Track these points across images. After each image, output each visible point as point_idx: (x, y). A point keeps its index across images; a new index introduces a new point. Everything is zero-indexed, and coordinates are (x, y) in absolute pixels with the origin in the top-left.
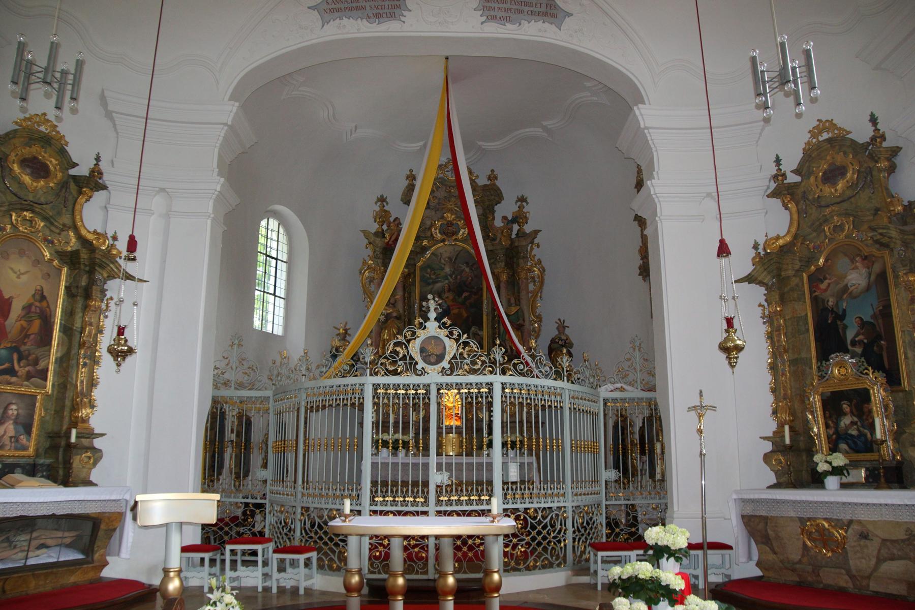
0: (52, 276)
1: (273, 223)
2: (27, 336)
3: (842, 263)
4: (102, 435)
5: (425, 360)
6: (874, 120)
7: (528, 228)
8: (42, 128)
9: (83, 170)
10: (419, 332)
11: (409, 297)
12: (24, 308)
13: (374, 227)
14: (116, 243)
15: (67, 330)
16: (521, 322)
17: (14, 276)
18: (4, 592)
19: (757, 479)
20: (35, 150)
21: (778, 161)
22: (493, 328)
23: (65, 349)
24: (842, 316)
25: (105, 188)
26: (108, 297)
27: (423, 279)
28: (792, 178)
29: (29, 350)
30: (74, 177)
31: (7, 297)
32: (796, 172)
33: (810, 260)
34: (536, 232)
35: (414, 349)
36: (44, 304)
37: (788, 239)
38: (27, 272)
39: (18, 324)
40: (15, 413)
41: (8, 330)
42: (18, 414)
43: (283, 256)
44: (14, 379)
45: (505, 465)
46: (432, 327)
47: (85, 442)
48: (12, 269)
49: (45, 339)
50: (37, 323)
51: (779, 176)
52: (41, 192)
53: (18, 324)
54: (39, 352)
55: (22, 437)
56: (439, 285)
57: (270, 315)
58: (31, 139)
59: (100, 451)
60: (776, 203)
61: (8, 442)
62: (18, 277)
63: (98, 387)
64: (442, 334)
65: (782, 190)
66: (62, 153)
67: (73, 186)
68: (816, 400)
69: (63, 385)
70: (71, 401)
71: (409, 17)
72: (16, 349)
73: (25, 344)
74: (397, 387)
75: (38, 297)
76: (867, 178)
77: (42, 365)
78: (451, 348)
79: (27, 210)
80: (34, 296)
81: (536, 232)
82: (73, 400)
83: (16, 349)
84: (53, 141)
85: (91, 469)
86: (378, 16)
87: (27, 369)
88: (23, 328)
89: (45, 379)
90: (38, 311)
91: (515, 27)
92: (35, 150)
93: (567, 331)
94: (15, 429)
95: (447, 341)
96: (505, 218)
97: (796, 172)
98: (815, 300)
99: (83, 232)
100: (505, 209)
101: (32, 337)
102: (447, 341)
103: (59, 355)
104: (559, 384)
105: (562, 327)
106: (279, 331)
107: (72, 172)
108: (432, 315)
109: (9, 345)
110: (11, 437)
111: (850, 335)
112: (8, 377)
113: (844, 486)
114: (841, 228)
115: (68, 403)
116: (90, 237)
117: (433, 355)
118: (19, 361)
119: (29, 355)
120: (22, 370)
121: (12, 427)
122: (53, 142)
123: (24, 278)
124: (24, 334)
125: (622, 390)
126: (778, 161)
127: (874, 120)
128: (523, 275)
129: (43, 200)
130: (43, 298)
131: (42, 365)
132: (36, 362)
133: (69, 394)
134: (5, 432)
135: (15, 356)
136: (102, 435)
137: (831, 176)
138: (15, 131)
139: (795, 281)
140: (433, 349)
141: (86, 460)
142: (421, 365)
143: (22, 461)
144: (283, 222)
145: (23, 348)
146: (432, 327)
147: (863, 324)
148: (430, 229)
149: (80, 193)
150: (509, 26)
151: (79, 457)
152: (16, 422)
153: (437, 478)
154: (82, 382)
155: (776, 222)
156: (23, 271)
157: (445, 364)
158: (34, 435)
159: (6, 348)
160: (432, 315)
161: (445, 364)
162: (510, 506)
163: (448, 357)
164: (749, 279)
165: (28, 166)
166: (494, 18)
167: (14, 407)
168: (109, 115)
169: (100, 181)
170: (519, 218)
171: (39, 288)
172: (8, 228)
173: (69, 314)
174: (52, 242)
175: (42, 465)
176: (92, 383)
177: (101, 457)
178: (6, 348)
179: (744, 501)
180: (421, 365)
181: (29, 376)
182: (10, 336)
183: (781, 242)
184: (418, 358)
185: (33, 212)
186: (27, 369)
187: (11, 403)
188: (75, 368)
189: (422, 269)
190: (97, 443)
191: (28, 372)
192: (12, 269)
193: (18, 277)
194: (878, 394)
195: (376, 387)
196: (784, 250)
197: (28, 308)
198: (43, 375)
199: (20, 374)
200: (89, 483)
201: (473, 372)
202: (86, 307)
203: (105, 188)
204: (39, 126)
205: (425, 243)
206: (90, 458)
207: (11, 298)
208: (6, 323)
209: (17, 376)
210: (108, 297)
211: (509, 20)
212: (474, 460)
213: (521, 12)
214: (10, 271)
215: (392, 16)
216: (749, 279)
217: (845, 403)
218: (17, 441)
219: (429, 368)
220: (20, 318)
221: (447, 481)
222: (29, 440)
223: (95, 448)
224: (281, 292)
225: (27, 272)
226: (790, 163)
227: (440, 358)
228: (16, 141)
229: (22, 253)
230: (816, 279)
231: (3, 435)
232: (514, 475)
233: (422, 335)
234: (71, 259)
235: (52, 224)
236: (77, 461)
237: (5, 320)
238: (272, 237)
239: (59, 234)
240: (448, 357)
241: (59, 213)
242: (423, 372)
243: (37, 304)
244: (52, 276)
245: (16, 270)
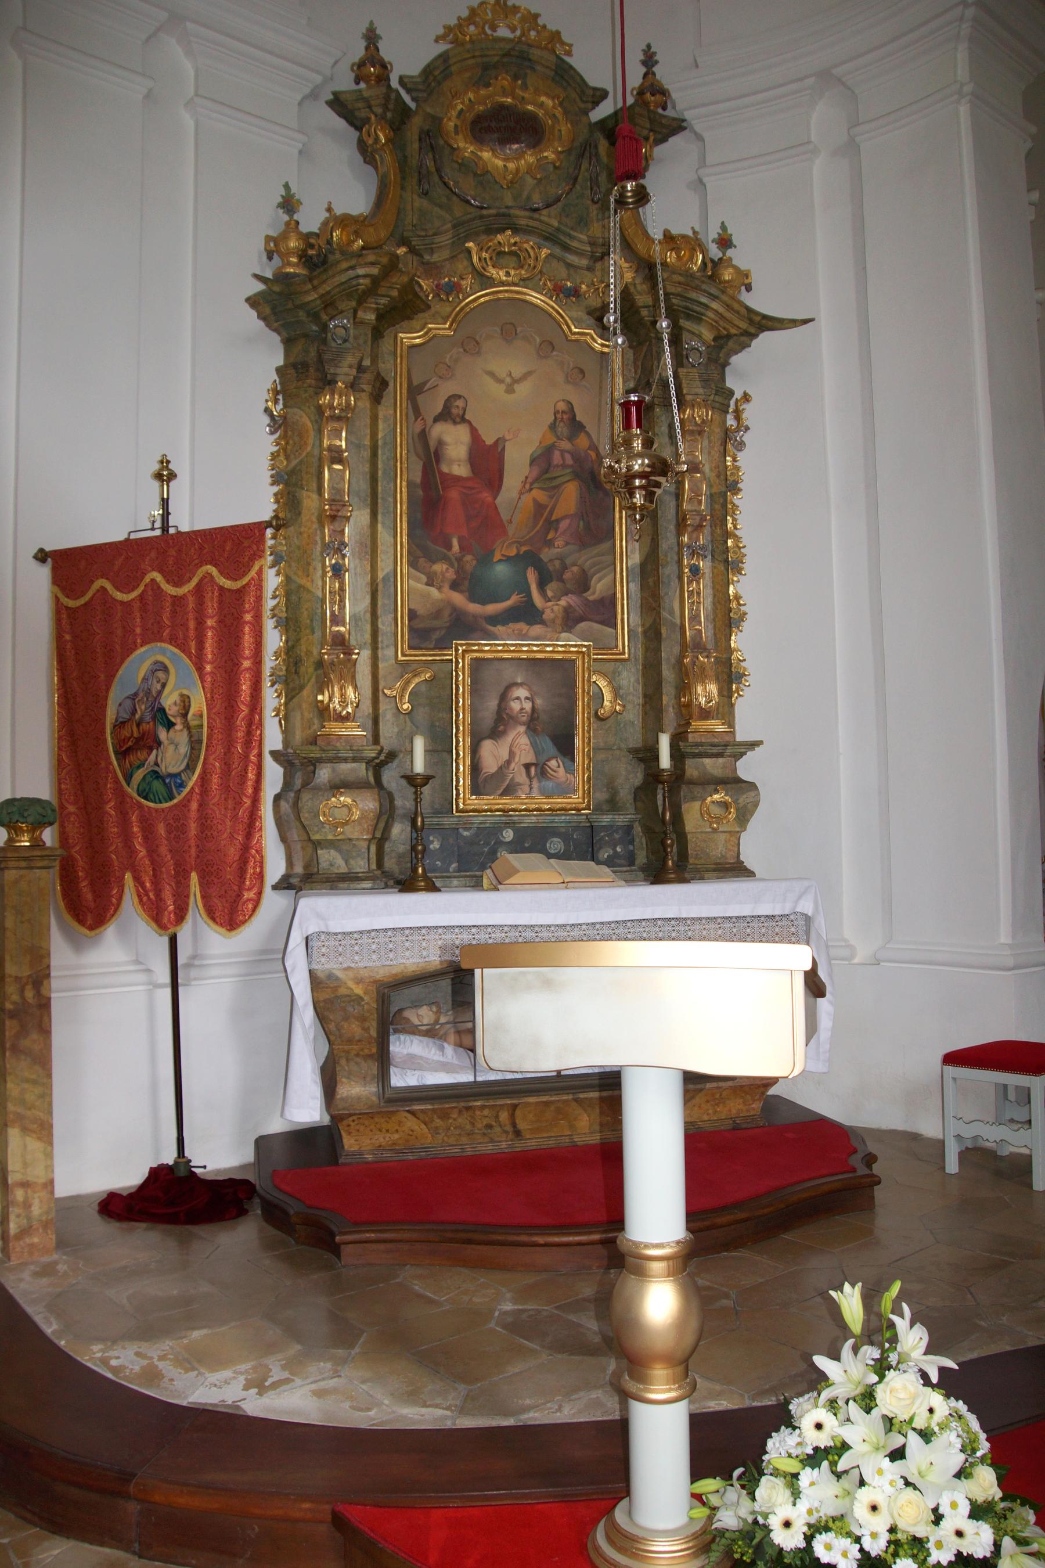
2: (551, 524)
4: (754, 745)
8: (503, 32)
12: (533, 461)
14: (730, 253)
17: (497, 390)
18: (518, 1133)
23: (647, 540)
25: (678, 126)
26: (738, 395)
29: (561, 558)
31: (489, 441)
36: (582, 442)
38: (525, 377)
39: (527, 499)
40: (528, 706)
41: (505, 516)
42: (533, 709)
44: (537, 629)
47: (712, 766)
48: (491, 374)
50: (571, 495)
52: (530, 181)
53: (527, 499)
54: (586, 558)
55: (553, 763)
58: (486, 67)
59: (752, 786)
61: (521, 777)
62: (510, 390)
63: (745, 625)
66: (564, 75)
69: (652, 635)
70: (685, 668)
72: (530, 559)
73: (550, 544)
75: (563, 429)
77: (598, 588)
79: (502, 230)
80: (553, 427)
82: (680, 662)
83: (530, 559)
84: (535, 53)
85: (736, 836)
87: (563, 603)
88: (539, 507)
89: (610, 621)
90: (569, 461)
92: (501, 92)
94: (534, 745)
101: (564, 525)
103: (636, 559)
109: (513, 552)
110: (527, 766)
112: (522, 626)
115: (668, 673)
118: (542, 585)
119: (565, 568)
120: (553, 609)
121: (524, 741)
123: (523, 389)
124: (544, 519)
129: (537, 201)
130: (576, 427)
131: (598, 588)
132: (583, 584)
133: (669, 651)
134: (512, 754)
135: (532, 576)
136: (754, 745)
138: (444, 57)
141: (716, 811)
143: (560, 820)
145: (546, 555)
151: (697, 805)
152: (533, 724)
154: (695, 618)
156: (517, 373)
158: (579, 758)
159: (508, 559)
165: (489, 130)
167: (522, 693)
169: (670, 112)
171: (562, 406)
172: (467, 283)
174: (575, 292)
175: (610, 828)
176: (727, 617)
177: (756, 805)
178: (508, 559)
181: (570, 621)
182: (511, 530)
185: (516, 230)
186: (563, 603)
187: (516, 684)
188: (675, 583)
190: (746, 768)
191: (567, 610)
192: (491, 374)
193: (510, 390)
197: (543, 460)
198: (604, 611)
199: (548, 615)
200: (735, 869)
203: (678, 126)
204: (494, 28)
206: (726, 805)
207: (500, 442)
208: (498, 501)
209: (543, 622)
210: (738, 395)
214: (488, 379)
218: (543, 773)
220: (528, 485)
222: (570, 771)
223: (739, 781)
225: (525, 377)
229: (509, 333)
231: (508, 762)
235: (566, 248)
236: (693, 816)
237: (495, 498)
239: (589, 269)
243: (565, 445)
245: (502, 373)
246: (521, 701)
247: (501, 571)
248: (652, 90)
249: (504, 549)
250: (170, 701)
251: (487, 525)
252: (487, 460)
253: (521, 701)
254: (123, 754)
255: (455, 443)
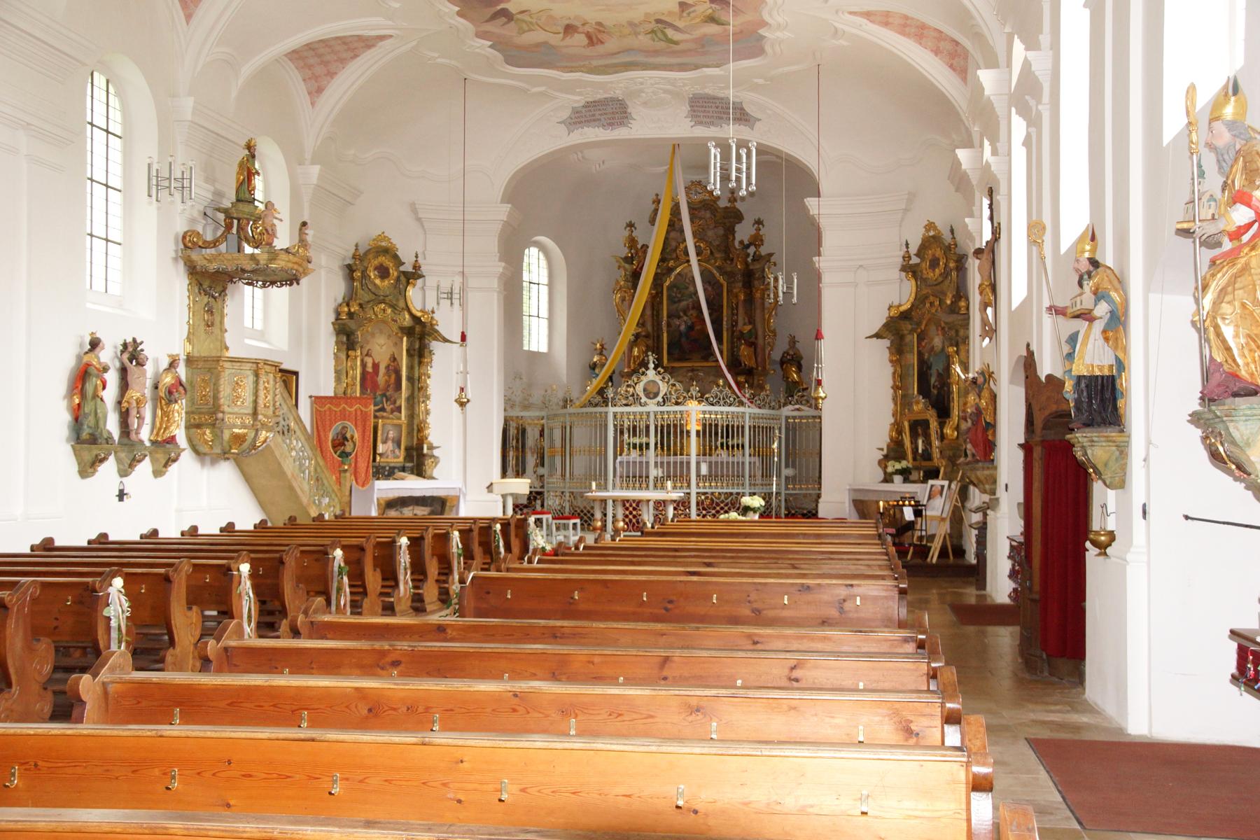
0: (398, 344)
1: (534, 251)
3: (933, 328)
5: (648, 396)
6: (952, 231)
7: (764, 251)
9: (408, 268)
10: (643, 377)
11: (658, 315)
13: (625, 252)
15: (410, 379)
16: (753, 340)
19: (869, 477)
20: (382, 259)
21: (907, 245)
22: (732, 343)
24: (929, 368)
27: (669, 297)
28: (915, 260)
30: (404, 273)
32: (917, 255)
33: (919, 324)
34: (771, 255)
35: (640, 389)
37: (908, 306)
43: (545, 280)
45: (698, 464)
46: (651, 374)
49: (398, 386)
50: (393, 376)
51: (907, 257)
54: (396, 395)
56: (684, 303)
57: (536, 338)
60: (904, 274)
64: (658, 379)
65: (909, 269)
66: (396, 257)
67: (403, 279)
68: (906, 424)
69: (412, 416)
71: (634, 124)
74: (628, 413)
76: (946, 274)
78: (664, 388)
81: (771, 255)
86: (611, 124)
91: (718, 129)
93: (798, 345)
95: (660, 383)
96: (741, 242)
97: (917, 255)
98: (920, 354)
99: (414, 312)
100: (743, 232)
102: (660, 383)
104: (741, 409)
105: (793, 341)
106: (544, 349)
107: (402, 269)
108: (651, 366)
111: (933, 380)
113: (906, 480)
114: (932, 304)
116: (419, 314)
117: (651, 393)
120: (388, 407)
122: (388, 251)
125: (798, 410)
126: (907, 245)
127: (952, 231)
128: (758, 295)
132: (395, 402)
133: (416, 422)
137: (934, 263)
139: (908, 338)
140: (652, 389)
142: (644, 399)
144: (542, 248)
146: (651, 374)
147: (939, 375)
148: (675, 250)
149: (408, 283)
150: (713, 128)
153: (654, 472)
155: (902, 293)
157: (659, 399)
160: (651, 366)
161: (659, 399)
162: (702, 490)
163: (661, 395)
164: (877, 336)
166: (701, 123)
168: (419, 219)
170: (757, 240)
173: (411, 368)
176: (427, 413)
179: (855, 490)
180: (644, 399)
183: (903, 308)
184: (642, 394)
189: (668, 288)
194: (934, 425)
195: (615, 415)
196: (905, 316)
197: (387, 367)
198: (399, 409)
200: (433, 478)
201: (677, 404)
202: (420, 363)
205: (671, 263)
211: (712, 124)
212: (714, 459)
213: (721, 118)
215: (622, 124)
216: (877, 336)
217: (919, 427)
219: (648, 401)
221: (660, 474)
224: (544, 312)
226: (913, 249)
227: (656, 395)
228: (371, 256)
229: (381, 332)
230: (920, 339)
232: (704, 470)
233: (644, 380)
234: (409, 332)
238: (535, 265)
240: (661, 395)
241: (398, 300)
242: (646, 404)
244: (398, 344)
246: (391, 434)
247: (379, 399)
248: (416, 267)
249: (379, 393)
250: (348, 436)
251: (375, 386)
252: (376, 366)
253: (391, 434)
254: (334, 447)
255: (369, 361)
